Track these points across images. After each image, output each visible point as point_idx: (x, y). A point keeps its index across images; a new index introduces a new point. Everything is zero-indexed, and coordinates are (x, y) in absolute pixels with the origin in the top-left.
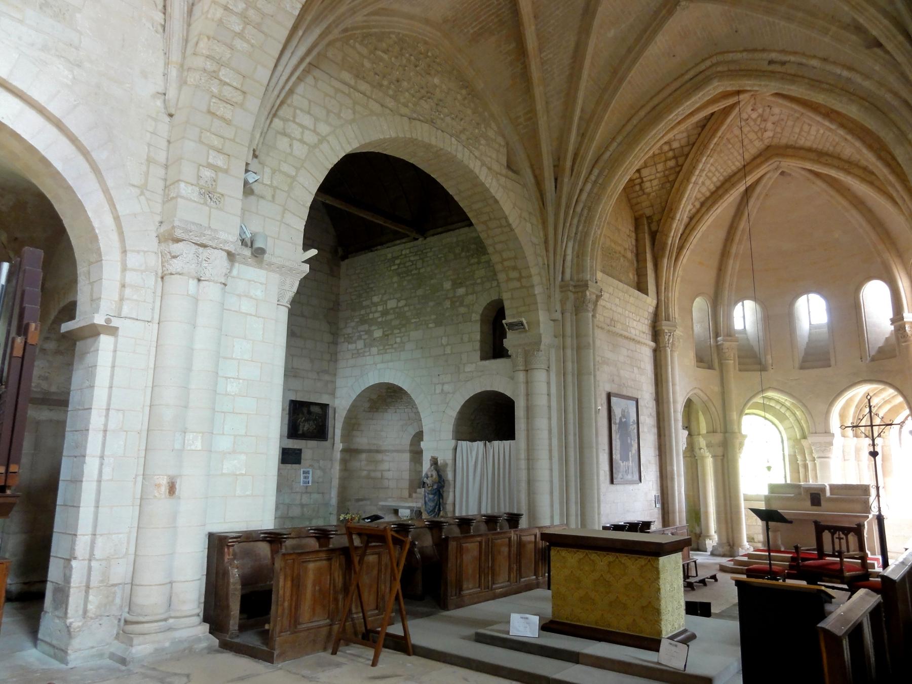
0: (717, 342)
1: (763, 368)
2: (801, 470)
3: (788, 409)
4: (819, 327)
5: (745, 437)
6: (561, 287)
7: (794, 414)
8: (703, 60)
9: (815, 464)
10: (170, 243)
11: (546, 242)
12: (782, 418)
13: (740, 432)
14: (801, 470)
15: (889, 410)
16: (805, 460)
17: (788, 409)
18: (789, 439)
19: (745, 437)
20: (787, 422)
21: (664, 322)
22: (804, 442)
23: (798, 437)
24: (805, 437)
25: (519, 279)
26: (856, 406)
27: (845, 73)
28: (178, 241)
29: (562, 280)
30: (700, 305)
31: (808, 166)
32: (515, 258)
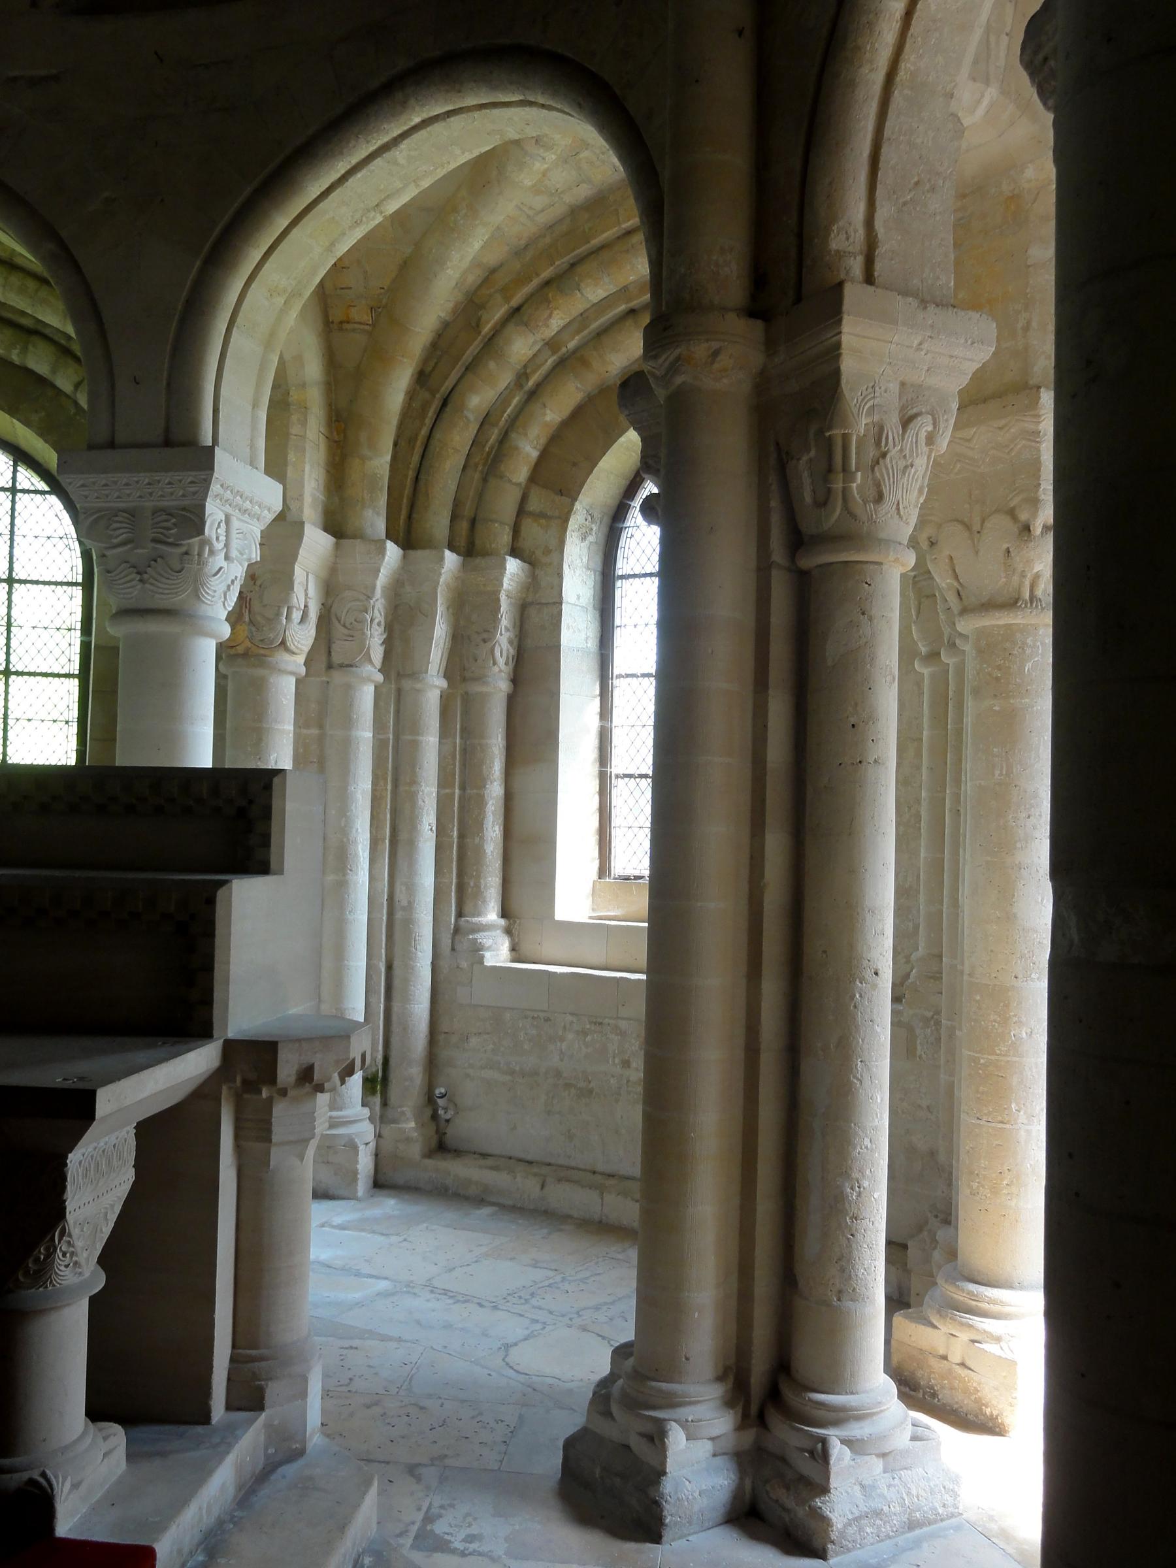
15: (577, 413)
26: (422, 377)
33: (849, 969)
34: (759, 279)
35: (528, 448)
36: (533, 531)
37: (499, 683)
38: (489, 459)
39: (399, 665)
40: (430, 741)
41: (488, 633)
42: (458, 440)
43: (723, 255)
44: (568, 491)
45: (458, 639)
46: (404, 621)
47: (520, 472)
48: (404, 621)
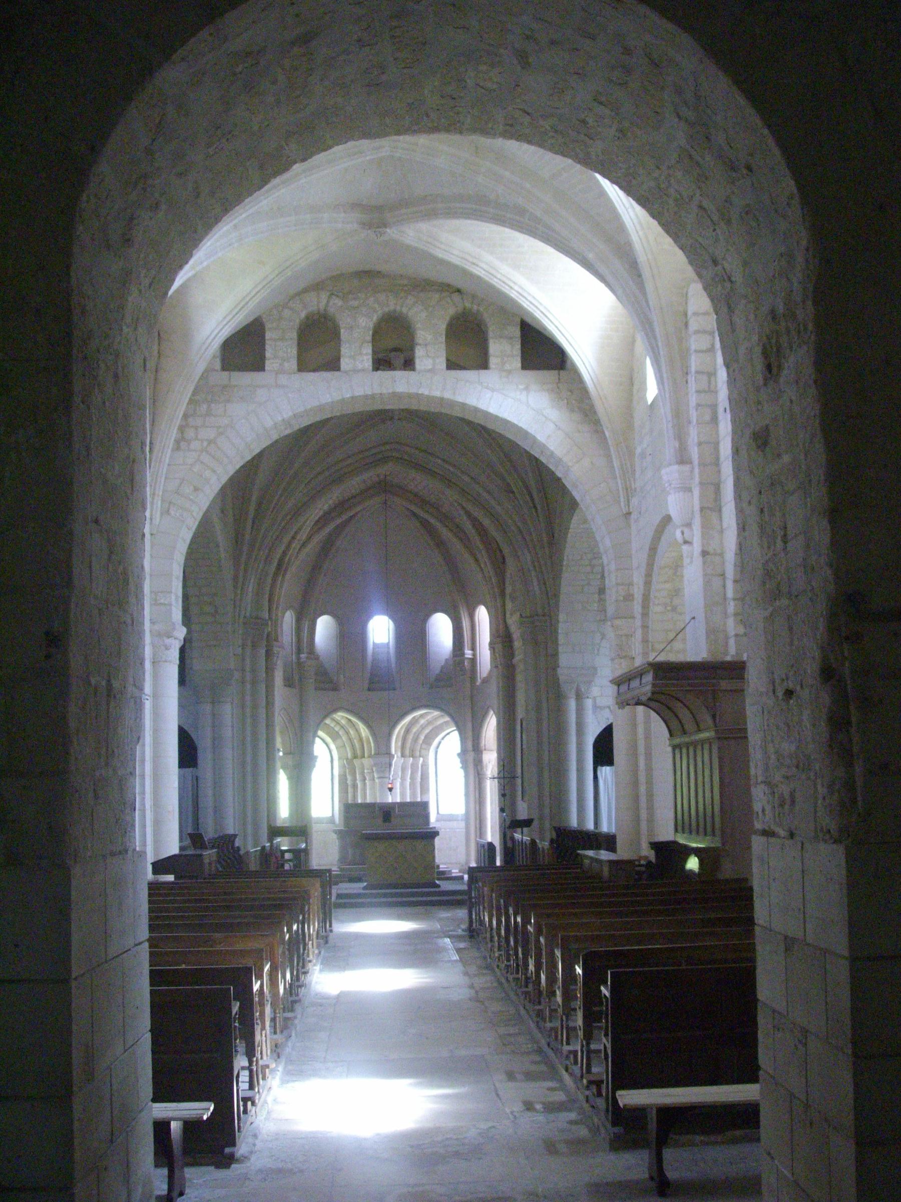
0: (299, 658)
1: (335, 689)
2: (350, 790)
3: (342, 727)
4: (382, 645)
5: (316, 757)
6: (245, 624)
7: (347, 733)
8: (384, 444)
9: (365, 784)
10: (165, 638)
11: (235, 578)
12: (335, 736)
13: (313, 754)
14: (350, 790)
16: (355, 779)
17: (342, 727)
18: (340, 758)
19: (316, 757)
20: (339, 741)
21: (275, 643)
22: (357, 762)
23: (350, 755)
24: (355, 757)
25: (213, 616)
27: (485, 495)
28: (169, 637)
29: (245, 617)
30: (288, 619)
31: (413, 508)
32: (215, 594)
33: (486, 818)
34: (473, 746)
35: (422, 737)
36: (423, 751)
37: (419, 780)
38: (416, 740)
39: (403, 779)
40: (408, 791)
41: (417, 771)
42: (410, 737)
43: (470, 744)
44: (430, 744)
45: (412, 773)
46: (404, 769)
47: (421, 742)
48: (404, 769)
